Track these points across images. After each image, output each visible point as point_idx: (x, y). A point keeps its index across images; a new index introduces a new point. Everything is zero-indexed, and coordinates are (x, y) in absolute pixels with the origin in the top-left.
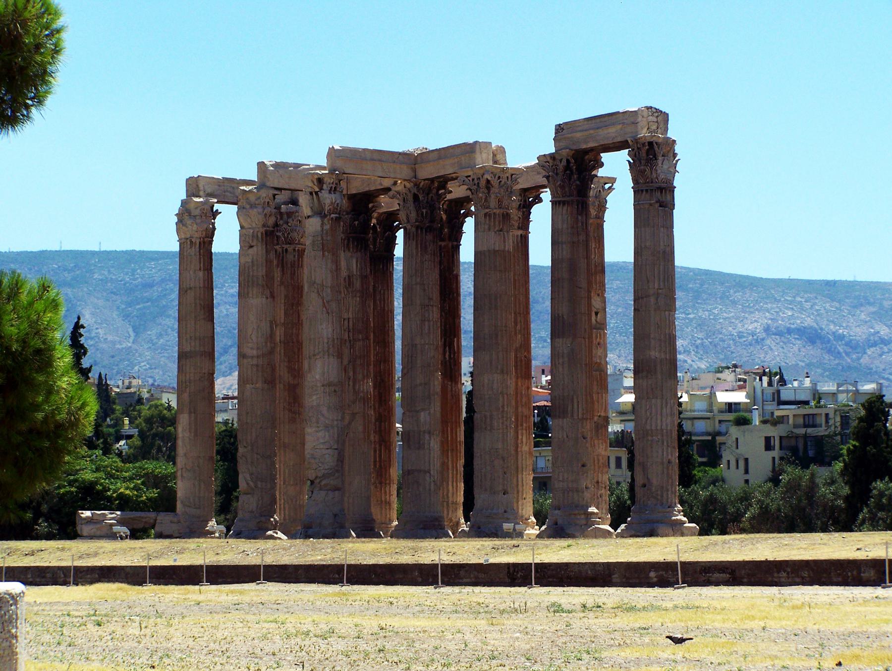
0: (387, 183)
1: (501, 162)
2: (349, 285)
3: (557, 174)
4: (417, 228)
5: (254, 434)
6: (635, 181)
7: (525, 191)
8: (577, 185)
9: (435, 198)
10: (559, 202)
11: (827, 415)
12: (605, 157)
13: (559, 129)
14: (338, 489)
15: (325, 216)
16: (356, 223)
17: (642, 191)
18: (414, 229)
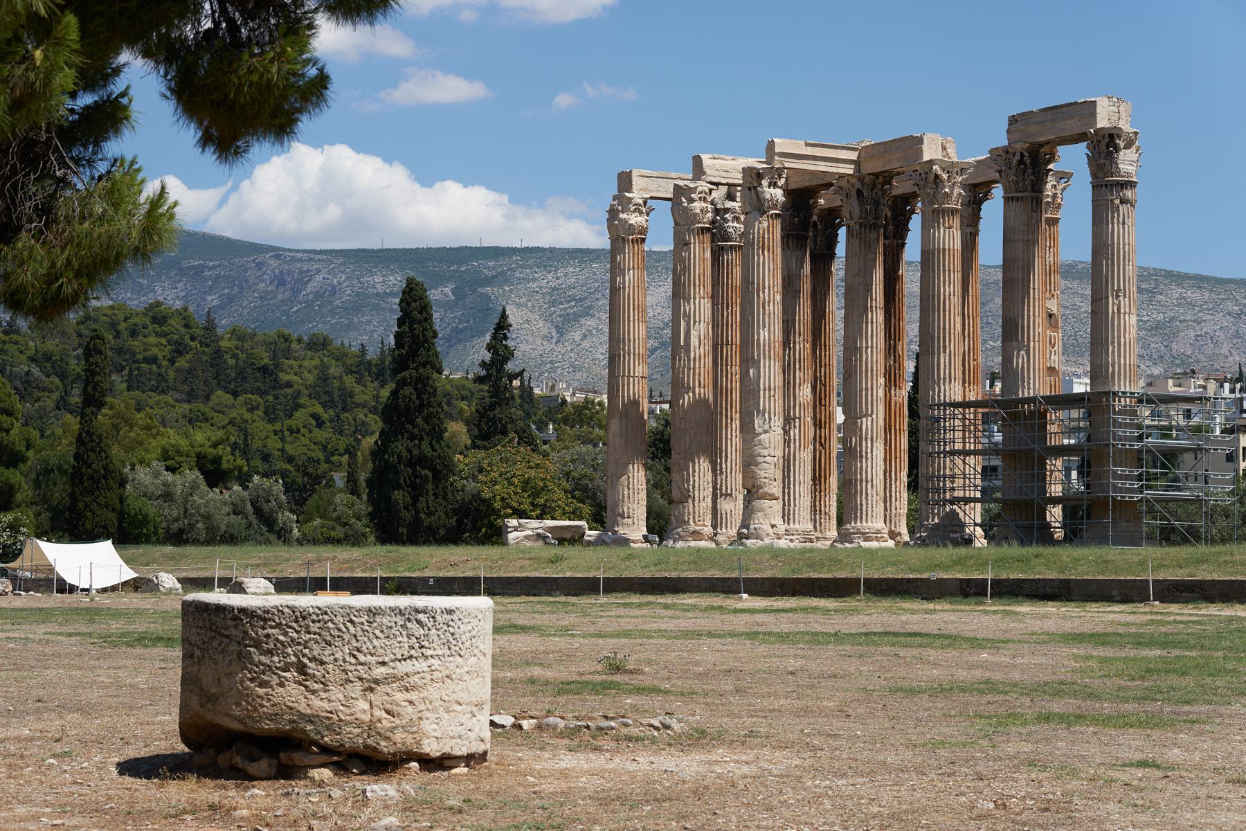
0: (827, 180)
1: (951, 155)
2: (789, 285)
3: (1010, 168)
4: (861, 225)
5: (688, 441)
6: (1094, 175)
7: (975, 187)
8: (1032, 180)
9: (880, 193)
10: (1013, 198)
12: (1061, 150)
13: (1013, 120)
14: (776, 499)
15: (765, 212)
16: (796, 219)
17: (1101, 186)
18: (857, 227)
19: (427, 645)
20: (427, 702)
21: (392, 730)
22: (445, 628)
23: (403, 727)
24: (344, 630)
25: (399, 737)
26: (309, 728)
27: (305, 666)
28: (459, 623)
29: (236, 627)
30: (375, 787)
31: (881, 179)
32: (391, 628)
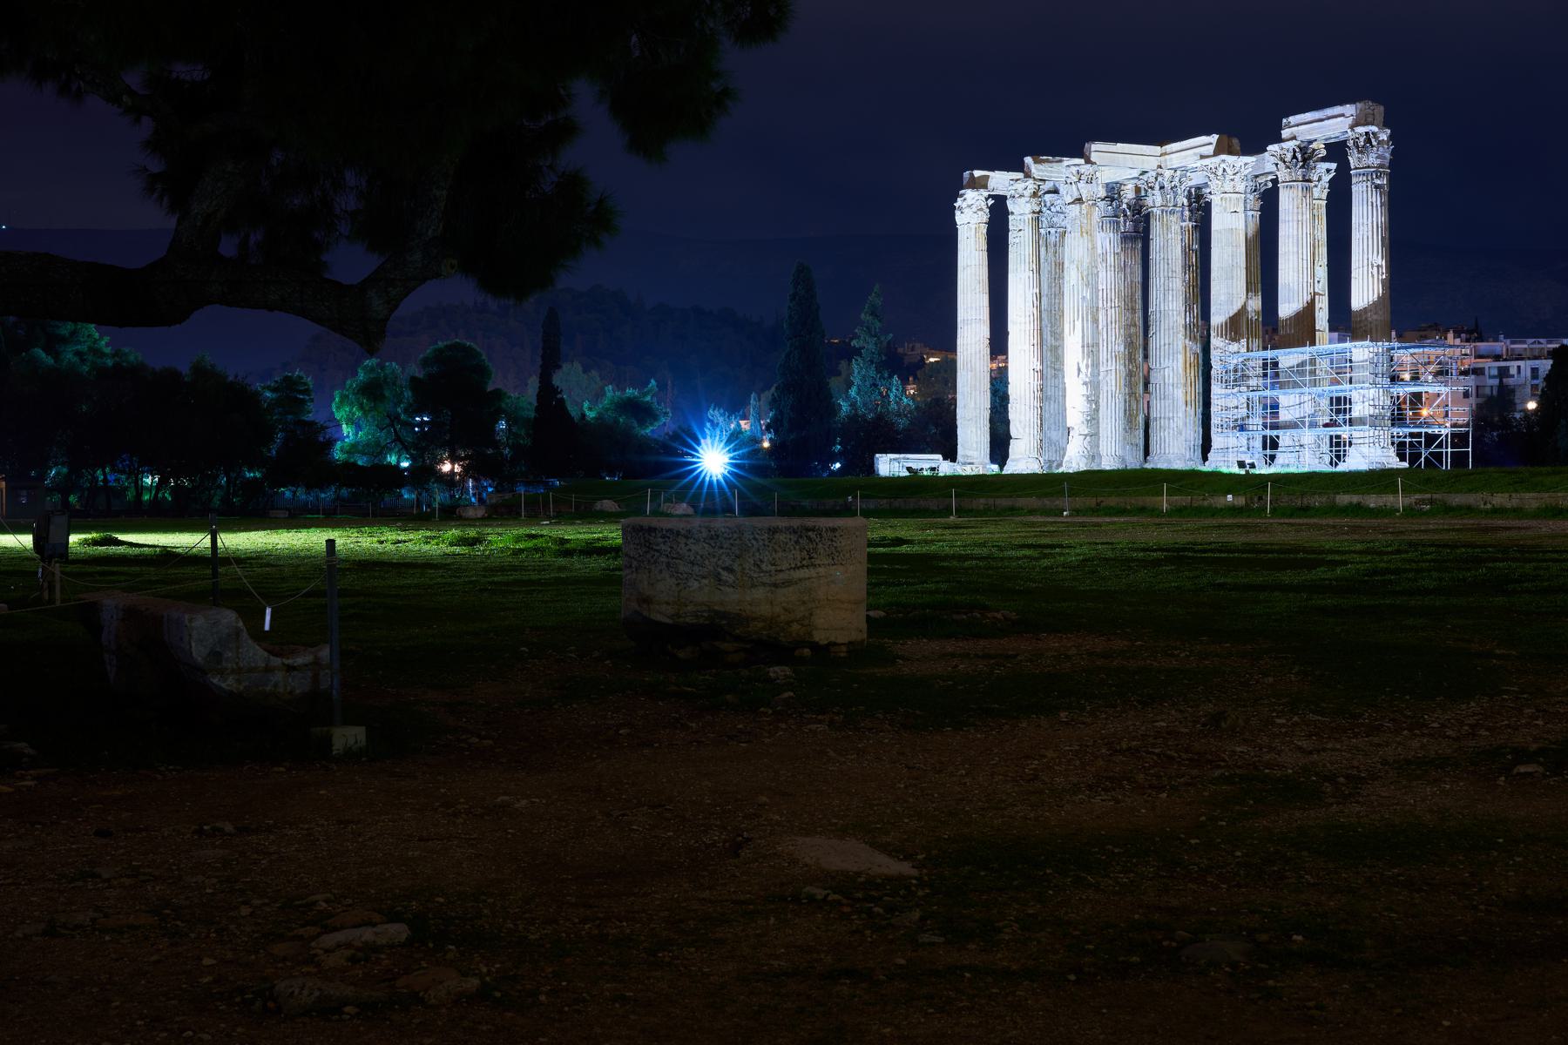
11: (1519, 367)
15: (1084, 203)
19: (816, 556)
20: (817, 602)
21: (789, 623)
22: (830, 543)
23: (797, 621)
24: (750, 545)
25: (795, 627)
26: (724, 622)
27: (719, 574)
28: (841, 539)
29: (664, 543)
30: (776, 669)
31: (1178, 172)
32: (787, 543)
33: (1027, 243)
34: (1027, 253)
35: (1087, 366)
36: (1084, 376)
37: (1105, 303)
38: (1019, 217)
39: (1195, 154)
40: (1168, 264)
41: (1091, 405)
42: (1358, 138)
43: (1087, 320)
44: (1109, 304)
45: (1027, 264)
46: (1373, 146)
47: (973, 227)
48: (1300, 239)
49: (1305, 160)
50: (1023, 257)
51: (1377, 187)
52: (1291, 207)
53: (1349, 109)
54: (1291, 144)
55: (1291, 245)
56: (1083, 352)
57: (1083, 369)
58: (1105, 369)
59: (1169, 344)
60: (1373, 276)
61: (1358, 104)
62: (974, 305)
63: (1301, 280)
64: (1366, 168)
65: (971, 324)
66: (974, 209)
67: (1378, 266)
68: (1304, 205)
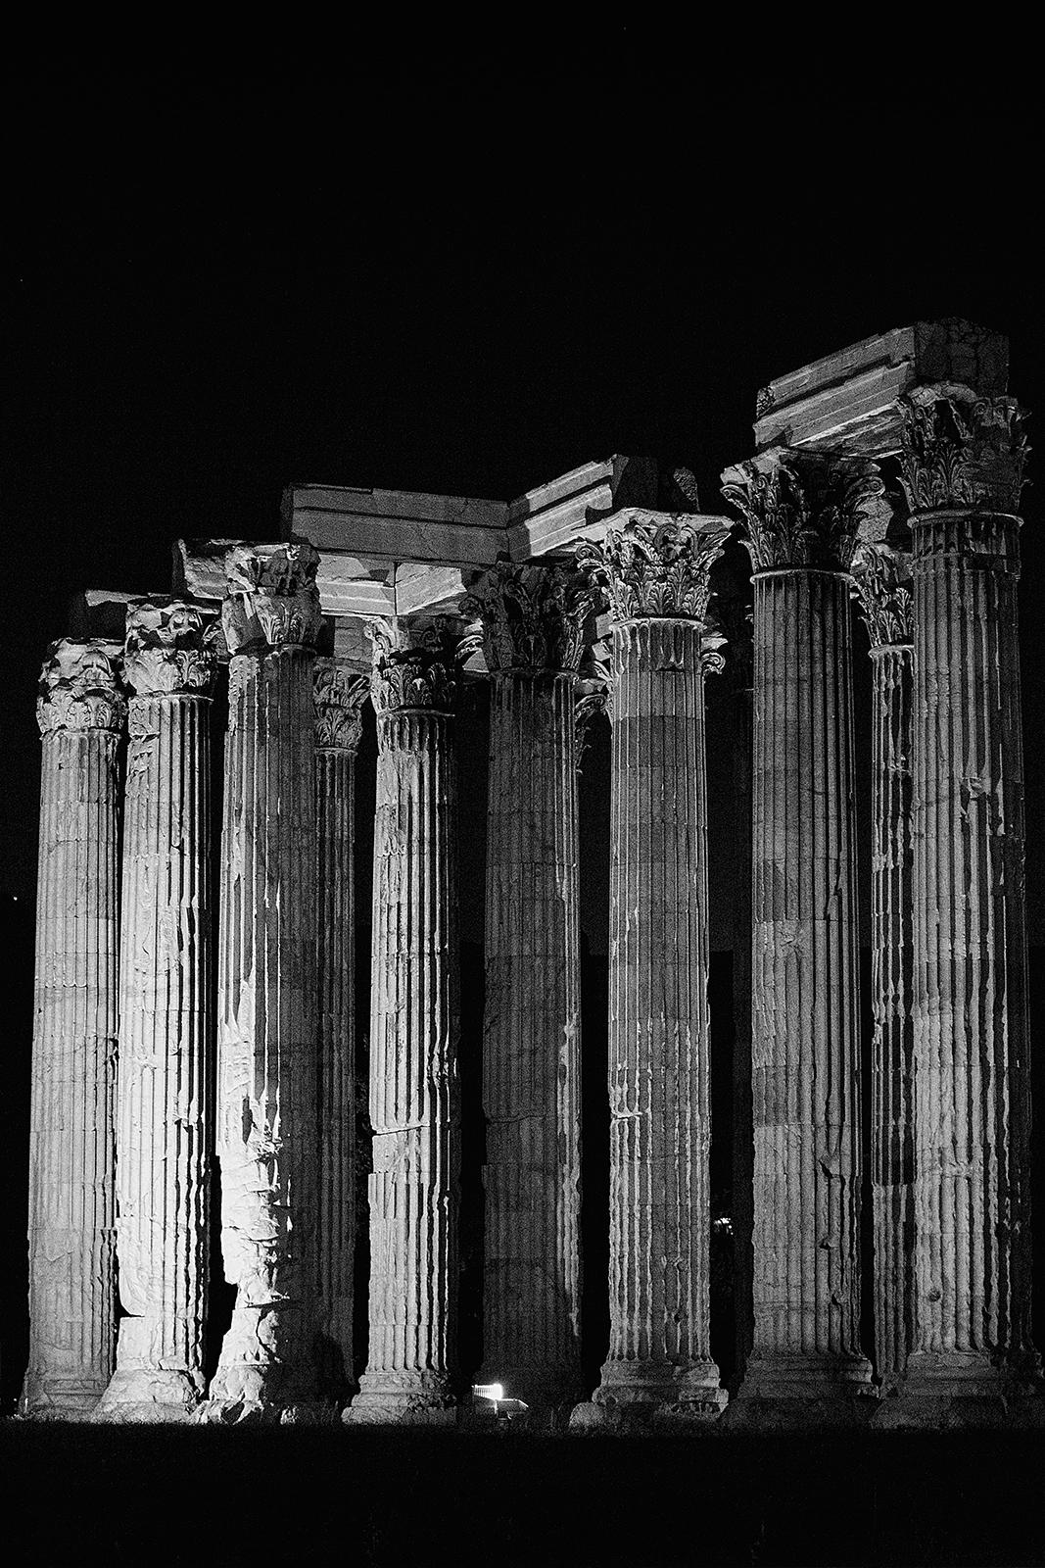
4: (517, 678)
16: (418, 681)
33: (165, 773)
34: (165, 799)
35: (270, 1108)
36: (262, 1138)
37: (404, 941)
38: (148, 701)
39: (576, 514)
40: (532, 827)
41: (282, 1222)
42: (919, 422)
43: (273, 979)
44: (415, 945)
45: (164, 830)
46: (961, 444)
47: (75, 738)
48: (806, 733)
49: (815, 506)
50: (153, 811)
51: (978, 563)
52: (780, 640)
53: (899, 340)
54: (769, 461)
55: (780, 748)
56: (259, 1070)
57: (260, 1119)
58: (403, 1126)
59: (533, 1052)
60: (966, 830)
61: (923, 325)
62: (71, 949)
63: (807, 851)
64: (942, 507)
65: (63, 1000)
66: (77, 691)
67: (980, 801)
68: (817, 635)
